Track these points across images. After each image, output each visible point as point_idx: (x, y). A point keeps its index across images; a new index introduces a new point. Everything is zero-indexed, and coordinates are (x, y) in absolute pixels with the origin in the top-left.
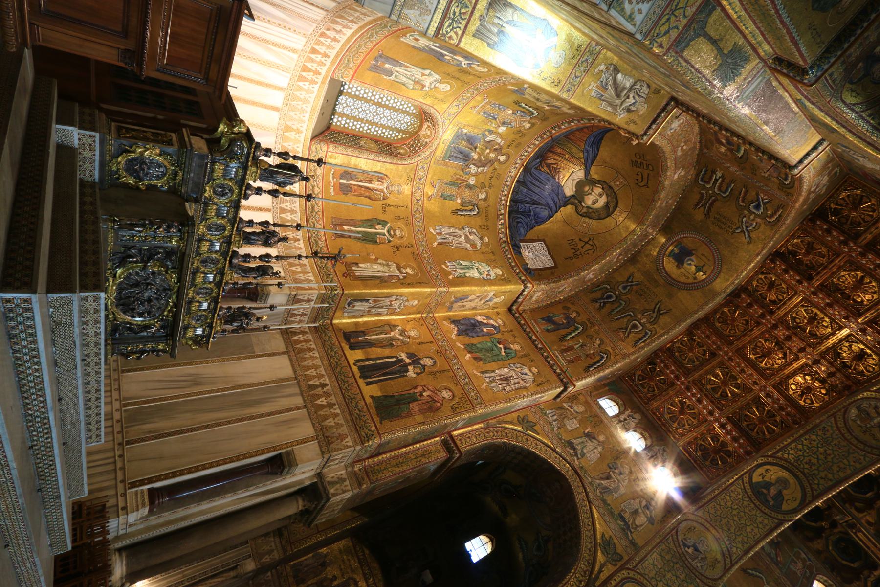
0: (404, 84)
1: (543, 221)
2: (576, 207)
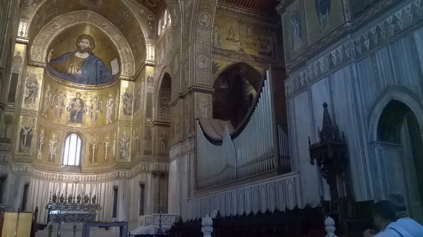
0: (56, 150)
1: (103, 63)
2: (92, 49)
